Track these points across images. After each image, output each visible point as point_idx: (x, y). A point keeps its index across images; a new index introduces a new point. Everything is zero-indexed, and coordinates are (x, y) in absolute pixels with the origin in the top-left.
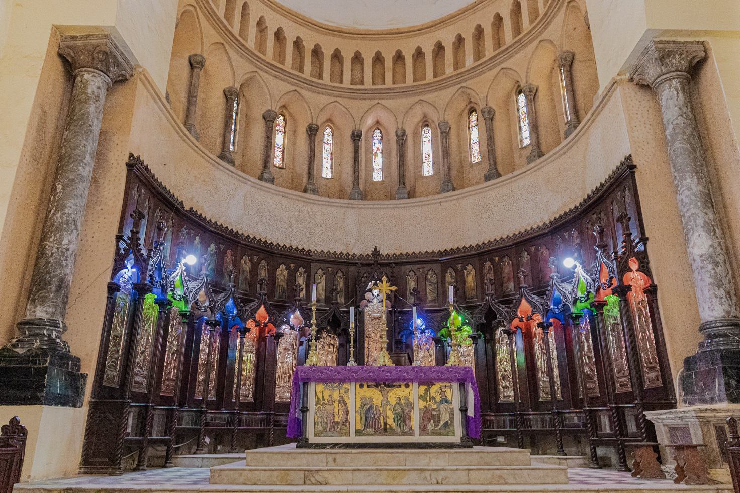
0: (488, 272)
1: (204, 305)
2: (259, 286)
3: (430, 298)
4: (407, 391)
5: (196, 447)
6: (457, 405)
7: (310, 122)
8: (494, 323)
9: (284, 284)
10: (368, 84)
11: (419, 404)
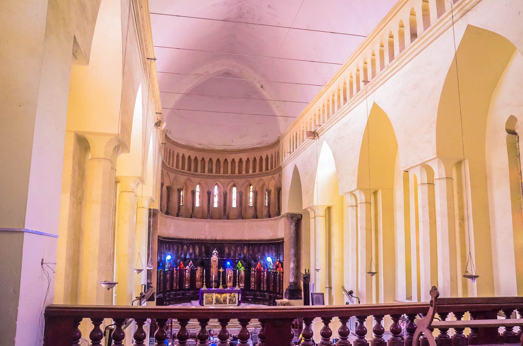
6: (237, 298)
10: (214, 173)
11: (228, 298)
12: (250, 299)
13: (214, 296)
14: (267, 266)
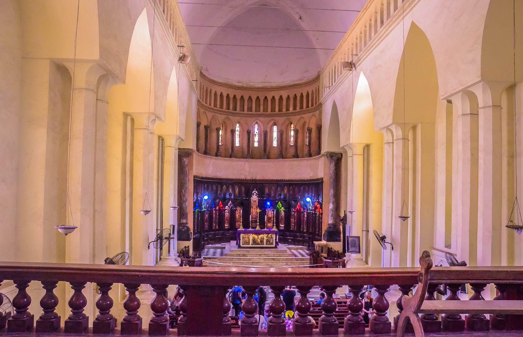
6: (274, 239)
7: (232, 128)
11: (265, 238)
12: (290, 240)
13: (251, 236)
14: (306, 207)
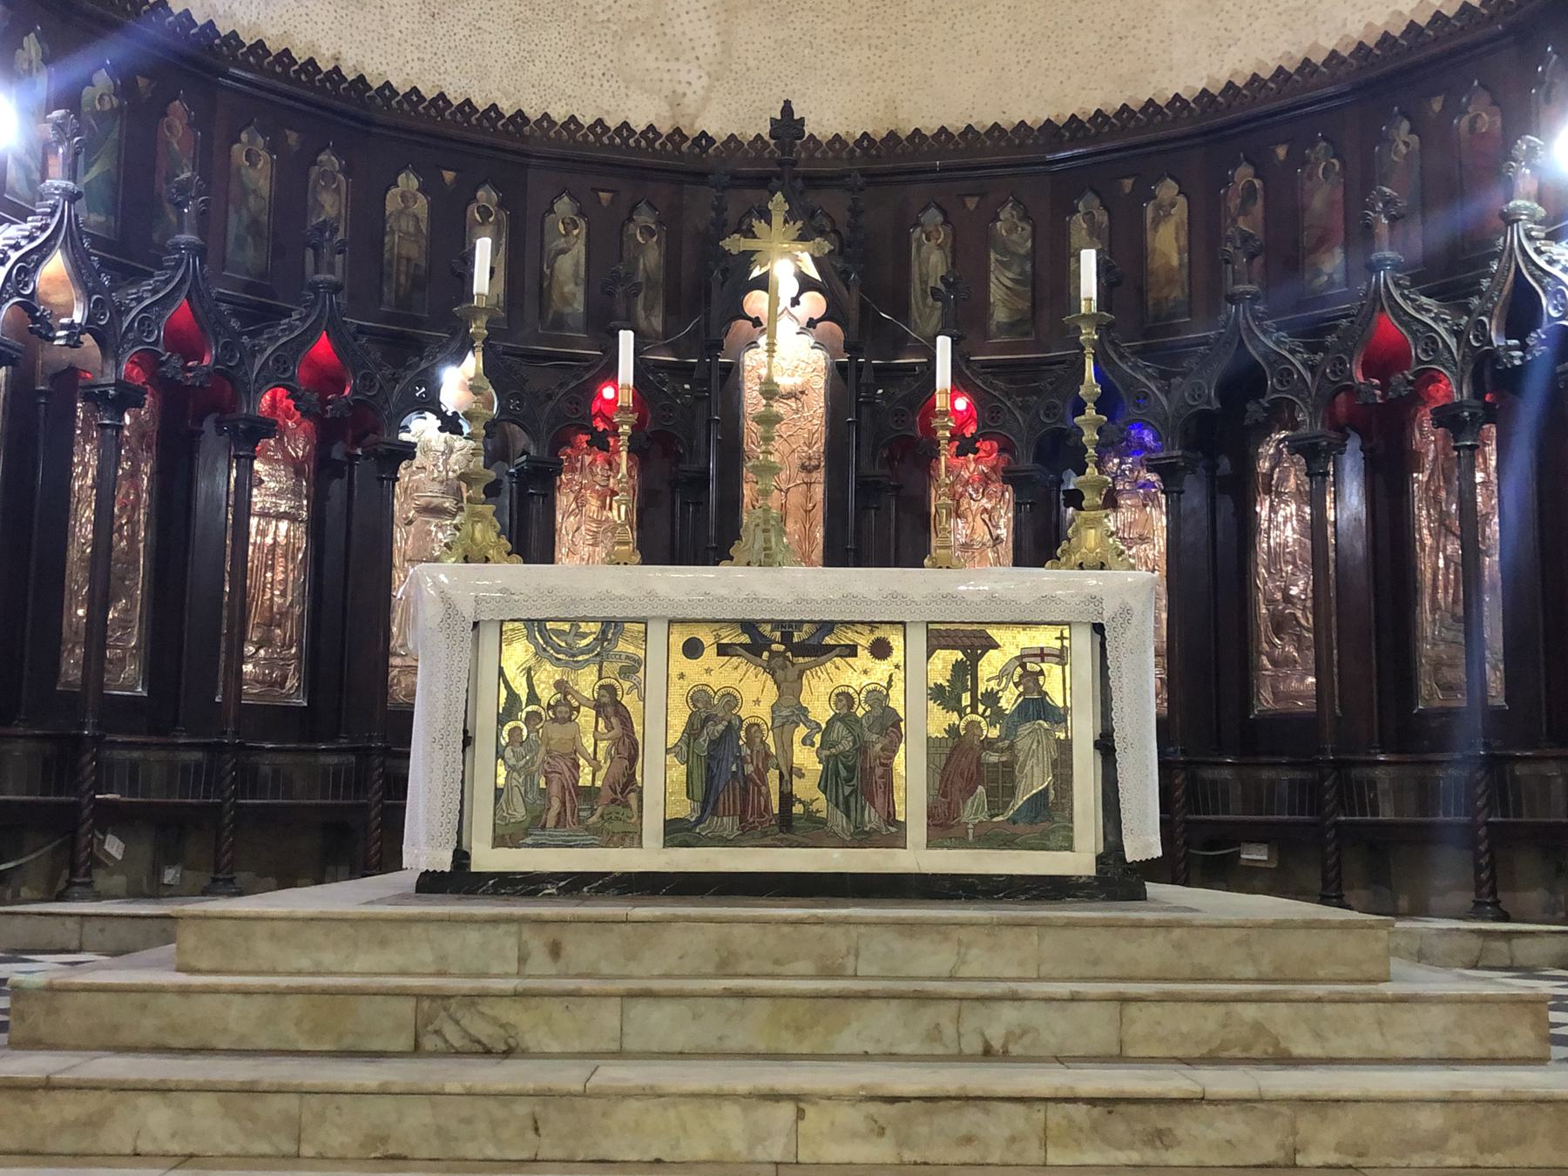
0: (1244, 209)
1: (65, 321)
2: (310, 253)
3: (1000, 315)
4: (880, 671)
5: (66, 873)
8: (1255, 411)
9: (414, 251)
